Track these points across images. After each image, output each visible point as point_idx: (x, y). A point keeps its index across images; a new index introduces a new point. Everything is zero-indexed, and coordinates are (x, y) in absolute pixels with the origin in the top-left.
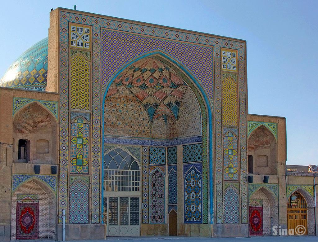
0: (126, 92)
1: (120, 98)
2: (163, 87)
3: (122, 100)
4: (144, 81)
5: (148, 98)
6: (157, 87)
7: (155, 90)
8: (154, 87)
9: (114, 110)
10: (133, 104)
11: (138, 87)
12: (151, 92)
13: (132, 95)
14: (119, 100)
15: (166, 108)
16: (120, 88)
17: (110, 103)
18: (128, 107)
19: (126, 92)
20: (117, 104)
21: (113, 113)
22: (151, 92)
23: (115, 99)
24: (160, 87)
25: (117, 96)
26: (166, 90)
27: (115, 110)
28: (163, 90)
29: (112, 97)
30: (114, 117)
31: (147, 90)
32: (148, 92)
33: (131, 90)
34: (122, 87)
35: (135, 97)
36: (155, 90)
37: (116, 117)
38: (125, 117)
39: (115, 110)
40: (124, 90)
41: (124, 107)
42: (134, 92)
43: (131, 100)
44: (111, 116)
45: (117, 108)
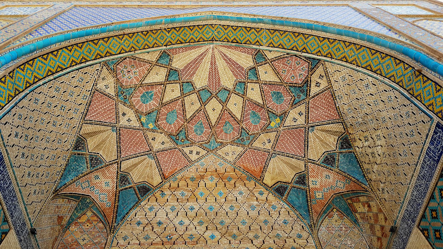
0: (210, 162)
1: (202, 177)
2: (283, 116)
5: (271, 165)
6: (273, 124)
7: (272, 135)
8: (266, 129)
9: (192, 209)
10: (241, 188)
11: (233, 143)
12: (268, 146)
14: (202, 183)
16: (193, 152)
17: (178, 193)
18: (229, 198)
20: (197, 193)
21: (191, 214)
22: (268, 146)
24: (278, 120)
25: (191, 172)
26: (295, 120)
27: (197, 207)
28: (288, 122)
30: (195, 223)
31: (257, 144)
32: (262, 146)
33: (219, 152)
34: (195, 149)
35: (240, 170)
36: (272, 135)
37: (201, 223)
38: (227, 221)
39: (197, 207)
41: (218, 198)
42: (230, 158)
43: (230, 179)
44: (187, 222)
45: (201, 201)
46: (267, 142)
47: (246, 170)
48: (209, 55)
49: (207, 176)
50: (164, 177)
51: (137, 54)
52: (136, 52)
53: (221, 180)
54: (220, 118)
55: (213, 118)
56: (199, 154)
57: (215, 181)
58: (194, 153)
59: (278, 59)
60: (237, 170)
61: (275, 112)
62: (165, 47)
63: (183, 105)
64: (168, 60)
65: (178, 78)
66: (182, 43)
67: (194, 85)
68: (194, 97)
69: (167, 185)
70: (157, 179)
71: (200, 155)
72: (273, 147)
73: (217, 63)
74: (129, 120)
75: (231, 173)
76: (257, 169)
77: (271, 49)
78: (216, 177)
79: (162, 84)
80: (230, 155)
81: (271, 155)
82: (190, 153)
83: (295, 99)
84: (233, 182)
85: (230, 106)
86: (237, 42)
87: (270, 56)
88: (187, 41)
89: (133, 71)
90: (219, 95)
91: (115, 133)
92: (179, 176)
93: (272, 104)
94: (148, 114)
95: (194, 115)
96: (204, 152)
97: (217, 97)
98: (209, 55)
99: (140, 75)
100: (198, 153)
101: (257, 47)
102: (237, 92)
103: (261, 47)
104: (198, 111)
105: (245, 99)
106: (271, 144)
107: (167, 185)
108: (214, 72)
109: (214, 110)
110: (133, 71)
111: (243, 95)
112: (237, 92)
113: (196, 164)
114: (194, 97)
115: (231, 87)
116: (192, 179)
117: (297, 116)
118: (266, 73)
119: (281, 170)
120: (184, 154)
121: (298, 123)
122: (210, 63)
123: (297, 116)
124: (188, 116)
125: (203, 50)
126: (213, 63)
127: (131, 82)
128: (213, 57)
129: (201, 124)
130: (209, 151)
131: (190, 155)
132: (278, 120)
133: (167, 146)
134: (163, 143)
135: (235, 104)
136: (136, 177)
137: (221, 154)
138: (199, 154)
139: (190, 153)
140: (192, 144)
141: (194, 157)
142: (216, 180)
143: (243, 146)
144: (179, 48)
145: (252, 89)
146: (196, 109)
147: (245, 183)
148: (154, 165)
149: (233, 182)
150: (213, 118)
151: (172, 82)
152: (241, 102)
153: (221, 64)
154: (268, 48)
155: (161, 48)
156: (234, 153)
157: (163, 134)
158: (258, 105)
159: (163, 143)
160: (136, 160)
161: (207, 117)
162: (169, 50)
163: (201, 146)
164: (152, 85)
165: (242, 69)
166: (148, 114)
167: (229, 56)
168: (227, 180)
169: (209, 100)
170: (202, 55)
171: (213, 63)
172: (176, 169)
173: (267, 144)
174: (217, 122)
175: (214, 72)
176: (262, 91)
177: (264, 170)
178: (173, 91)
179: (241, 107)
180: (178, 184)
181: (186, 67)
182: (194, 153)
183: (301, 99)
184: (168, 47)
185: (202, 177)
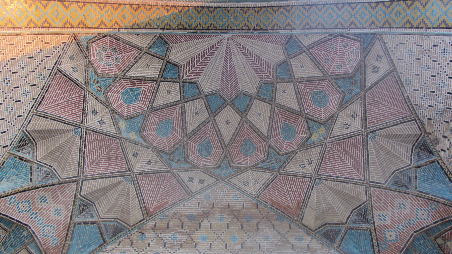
1: (206, 215)
3: (216, 223)
4: (264, 138)
5: (314, 197)
6: (314, 138)
7: (315, 153)
13: (248, 202)
14: (205, 223)
15: (398, 201)
19: (221, 194)
22: (309, 169)
23: (185, 220)
25: (190, 207)
28: (337, 131)
29: (170, 213)
31: (292, 168)
33: (234, 181)
34: (198, 175)
36: (315, 153)
40: (209, 187)
46: (306, 164)
47: (276, 206)
48: (223, 49)
49: (214, 214)
50: (147, 213)
51: (122, 33)
52: (121, 30)
53: (235, 220)
54: (237, 134)
55: (227, 133)
56: (202, 183)
57: (226, 221)
58: (196, 181)
59: (317, 44)
60: (261, 206)
61: (316, 119)
62: (161, 31)
63: (183, 113)
64: (165, 49)
65: (177, 76)
66: (185, 29)
67: (200, 88)
68: (200, 103)
69: (151, 224)
70: (136, 215)
71: (205, 184)
72: (317, 170)
73: (234, 59)
74: (101, 122)
75: (252, 211)
76: (293, 205)
77: (307, 31)
78: (229, 215)
79: (155, 81)
80: (251, 185)
81: (313, 181)
82: (189, 181)
83: (345, 96)
84: (254, 222)
85: (252, 116)
86: (261, 29)
87: (307, 42)
88: (193, 27)
89: (114, 57)
90: (236, 102)
91: (78, 137)
92: (170, 213)
93: (311, 109)
94: (131, 118)
95: (198, 129)
96: (211, 181)
97: (232, 104)
98: (223, 49)
99: (123, 63)
100: (202, 182)
101: (289, 31)
102: (262, 97)
103: (294, 32)
104: (204, 123)
105: (273, 105)
106: (314, 165)
107: (151, 224)
108: (229, 71)
109: (228, 123)
110: (114, 57)
111: (271, 101)
112: (262, 97)
113: (198, 196)
114: (200, 103)
115: (253, 91)
116: (191, 218)
117: (349, 120)
118: (302, 66)
119: (328, 203)
120: (180, 182)
121: (351, 129)
122: (223, 59)
123: (349, 120)
124: (190, 129)
125: (214, 40)
126: (228, 59)
127: (110, 70)
128: (228, 50)
129: (209, 142)
130: (218, 178)
131: (189, 184)
132: (322, 130)
133: (154, 167)
134: (149, 163)
135: (259, 115)
136: (104, 210)
137: (237, 183)
138: (202, 183)
139: (189, 181)
140: (194, 167)
141: (195, 186)
142: (228, 219)
143: (270, 170)
144: (181, 35)
145: (284, 92)
146: (200, 121)
147: (273, 225)
148: (133, 193)
149: (254, 222)
150: (227, 133)
151: (169, 80)
152: (268, 111)
153: (239, 60)
154: (303, 31)
155: (156, 31)
156: (256, 182)
157: (150, 150)
158: (293, 112)
159: (149, 163)
160: (106, 182)
161: (218, 132)
162: (167, 35)
163: (206, 171)
164: (140, 80)
165: (269, 66)
166: (131, 118)
167: (250, 50)
168: (245, 220)
169: (220, 108)
170: (213, 48)
171: (228, 59)
172: (167, 203)
173: (308, 166)
174: (233, 140)
175: (229, 71)
176: (298, 92)
177: (302, 205)
178: (169, 92)
179: (268, 118)
180: (168, 224)
181: (189, 62)
182: (196, 181)
183: (354, 93)
184: (166, 31)
185: (206, 215)
